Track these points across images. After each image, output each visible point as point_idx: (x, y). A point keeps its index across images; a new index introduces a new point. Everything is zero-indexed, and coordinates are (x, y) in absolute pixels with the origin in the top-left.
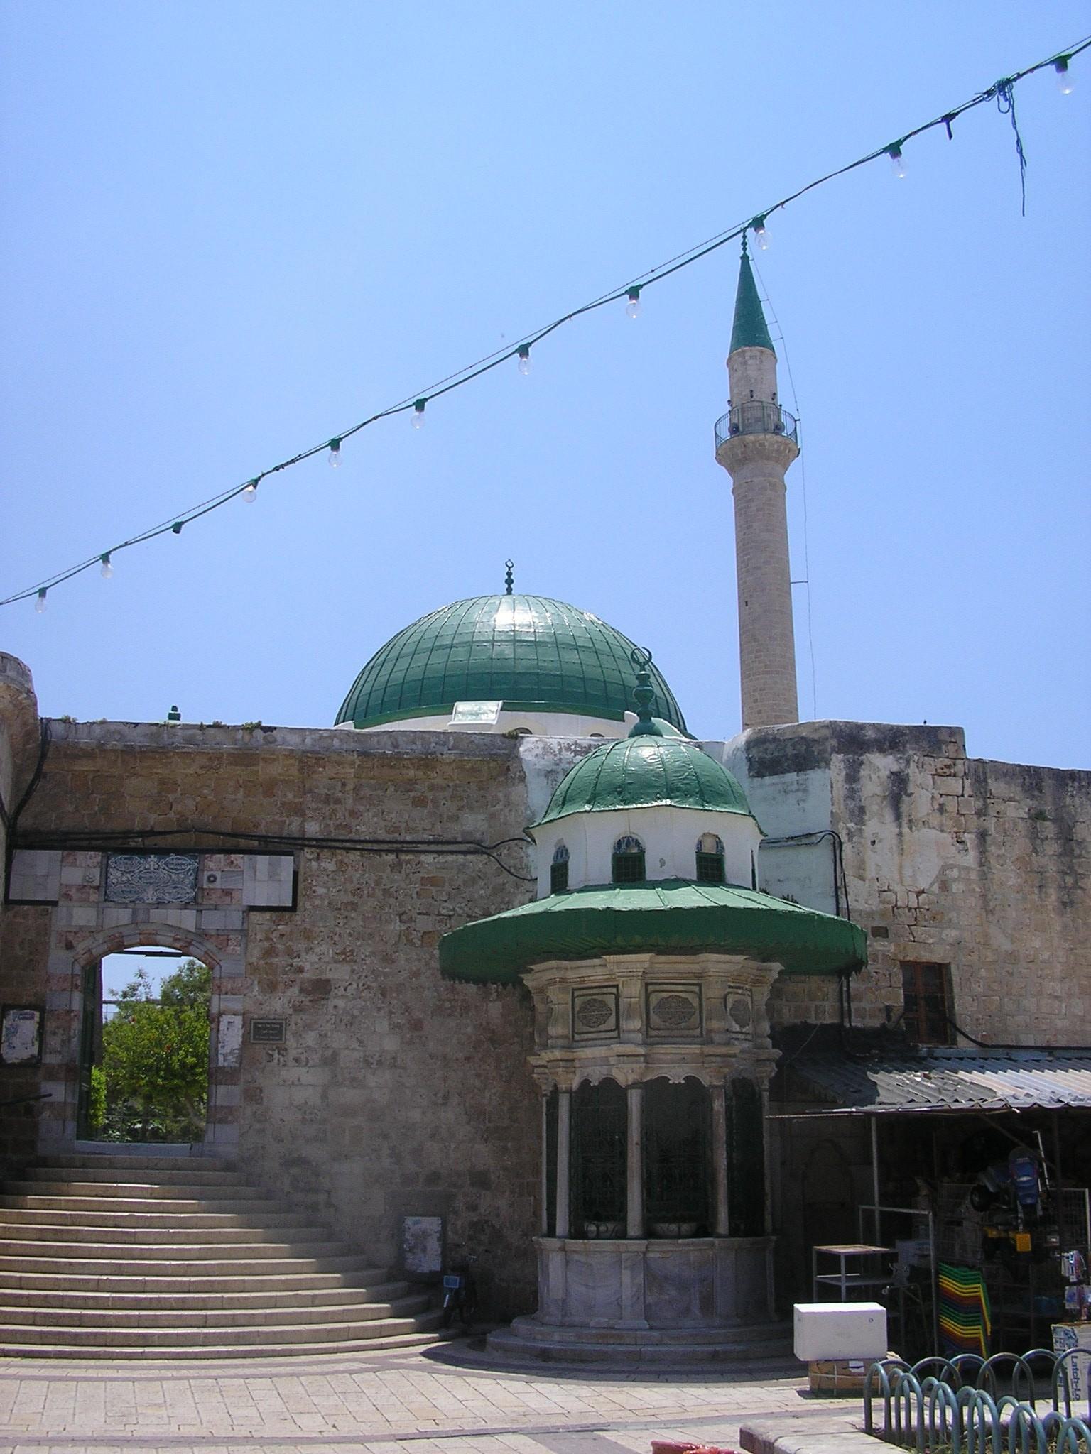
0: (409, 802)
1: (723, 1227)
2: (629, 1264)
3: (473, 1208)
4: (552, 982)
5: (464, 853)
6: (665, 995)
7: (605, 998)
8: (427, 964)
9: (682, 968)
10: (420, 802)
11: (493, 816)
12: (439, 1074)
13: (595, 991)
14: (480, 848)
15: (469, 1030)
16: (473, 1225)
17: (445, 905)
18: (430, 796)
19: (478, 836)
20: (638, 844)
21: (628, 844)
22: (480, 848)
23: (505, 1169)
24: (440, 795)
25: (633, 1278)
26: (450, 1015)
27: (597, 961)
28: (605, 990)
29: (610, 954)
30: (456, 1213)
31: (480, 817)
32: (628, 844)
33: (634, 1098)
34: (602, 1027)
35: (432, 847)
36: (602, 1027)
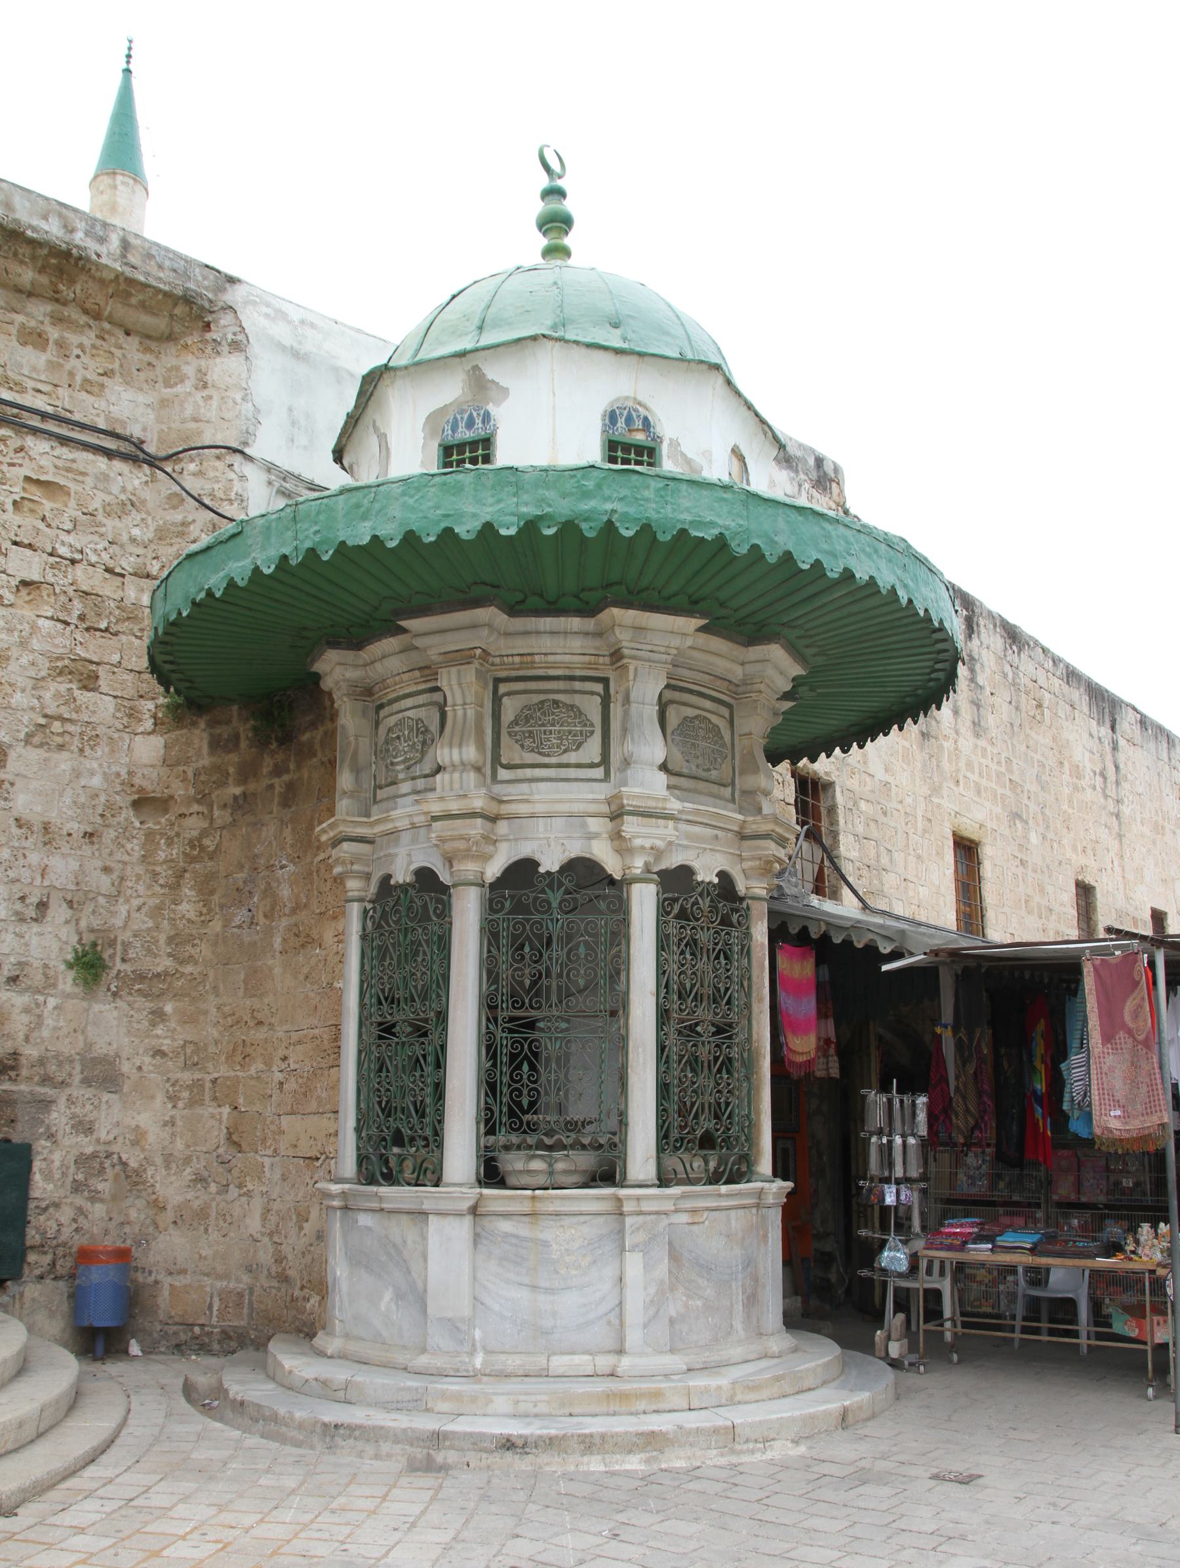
0: (15, 332)
1: (765, 1165)
2: (641, 1237)
3: (85, 1127)
4: (461, 658)
5: (109, 454)
6: (690, 712)
7: (577, 700)
8: (23, 644)
9: (722, 666)
10: (34, 338)
11: (164, 403)
12: (34, 858)
13: (561, 685)
14: (135, 454)
15: (96, 781)
16: (82, 1161)
17: (70, 539)
18: (53, 333)
19: (136, 431)
20: (647, 425)
21: (629, 420)
22: (135, 454)
23: (159, 1053)
24: (73, 338)
25: (647, 1267)
26: (61, 747)
27: (575, 623)
28: (577, 685)
29: (627, 604)
30: (51, 1136)
31: (141, 398)
32: (629, 420)
33: (644, 904)
34: (572, 757)
35: (51, 426)
36: (572, 757)
